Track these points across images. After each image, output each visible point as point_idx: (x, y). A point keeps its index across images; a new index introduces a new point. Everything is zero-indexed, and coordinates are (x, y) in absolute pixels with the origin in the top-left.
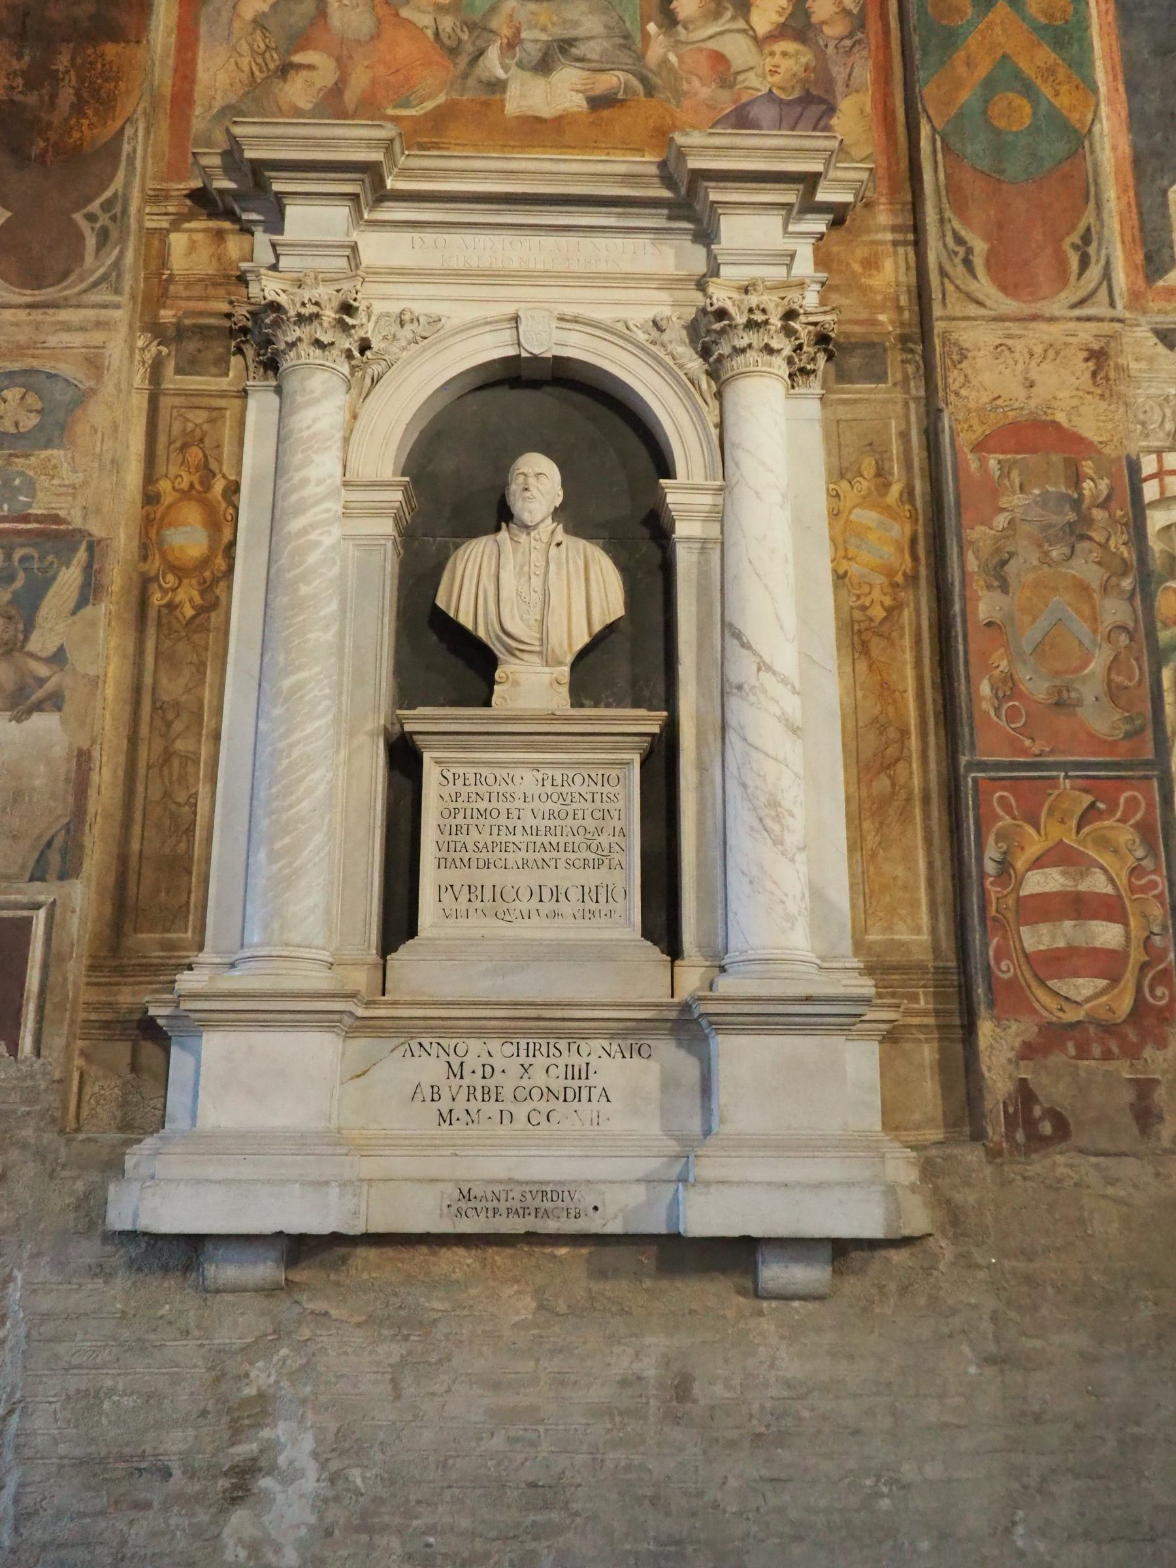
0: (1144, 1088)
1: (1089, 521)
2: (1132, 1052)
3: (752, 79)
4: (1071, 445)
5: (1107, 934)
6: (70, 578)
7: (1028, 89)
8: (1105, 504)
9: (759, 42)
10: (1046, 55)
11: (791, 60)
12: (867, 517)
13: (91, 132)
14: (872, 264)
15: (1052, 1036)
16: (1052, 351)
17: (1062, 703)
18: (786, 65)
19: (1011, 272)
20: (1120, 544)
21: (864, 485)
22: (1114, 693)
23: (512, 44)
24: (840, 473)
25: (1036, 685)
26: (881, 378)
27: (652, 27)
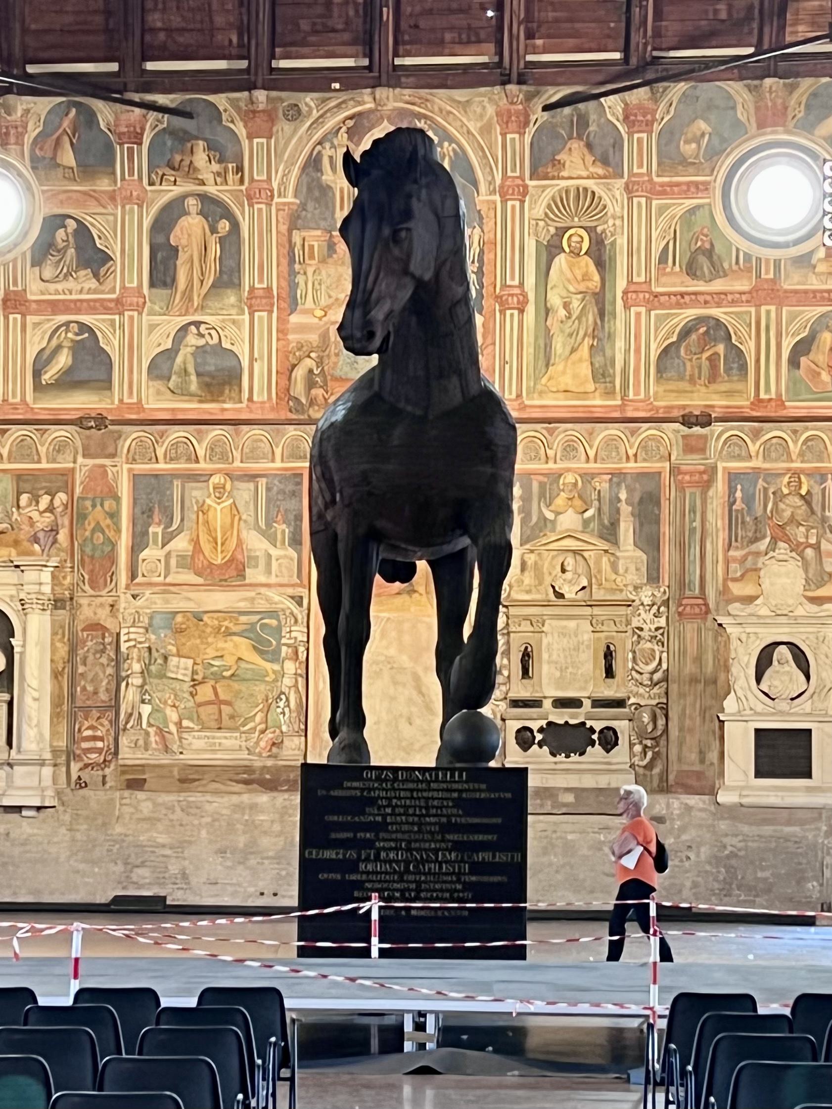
0: (104, 777)
1: (105, 648)
2: (103, 769)
3: (38, 524)
4: (104, 629)
5: (100, 744)
7: (103, 532)
8: (110, 644)
9: (41, 513)
10: (108, 521)
11: (48, 518)
12: (59, 645)
14: (64, 578)
16: (102, 605)
17: (96, 693)
18: (48, 520)
20: (113, 655)
21: (59, 637)
22: (107, 690)
24: (54, 634)
25: (90, 688)
26: (64, 608)
27: (14, 510)
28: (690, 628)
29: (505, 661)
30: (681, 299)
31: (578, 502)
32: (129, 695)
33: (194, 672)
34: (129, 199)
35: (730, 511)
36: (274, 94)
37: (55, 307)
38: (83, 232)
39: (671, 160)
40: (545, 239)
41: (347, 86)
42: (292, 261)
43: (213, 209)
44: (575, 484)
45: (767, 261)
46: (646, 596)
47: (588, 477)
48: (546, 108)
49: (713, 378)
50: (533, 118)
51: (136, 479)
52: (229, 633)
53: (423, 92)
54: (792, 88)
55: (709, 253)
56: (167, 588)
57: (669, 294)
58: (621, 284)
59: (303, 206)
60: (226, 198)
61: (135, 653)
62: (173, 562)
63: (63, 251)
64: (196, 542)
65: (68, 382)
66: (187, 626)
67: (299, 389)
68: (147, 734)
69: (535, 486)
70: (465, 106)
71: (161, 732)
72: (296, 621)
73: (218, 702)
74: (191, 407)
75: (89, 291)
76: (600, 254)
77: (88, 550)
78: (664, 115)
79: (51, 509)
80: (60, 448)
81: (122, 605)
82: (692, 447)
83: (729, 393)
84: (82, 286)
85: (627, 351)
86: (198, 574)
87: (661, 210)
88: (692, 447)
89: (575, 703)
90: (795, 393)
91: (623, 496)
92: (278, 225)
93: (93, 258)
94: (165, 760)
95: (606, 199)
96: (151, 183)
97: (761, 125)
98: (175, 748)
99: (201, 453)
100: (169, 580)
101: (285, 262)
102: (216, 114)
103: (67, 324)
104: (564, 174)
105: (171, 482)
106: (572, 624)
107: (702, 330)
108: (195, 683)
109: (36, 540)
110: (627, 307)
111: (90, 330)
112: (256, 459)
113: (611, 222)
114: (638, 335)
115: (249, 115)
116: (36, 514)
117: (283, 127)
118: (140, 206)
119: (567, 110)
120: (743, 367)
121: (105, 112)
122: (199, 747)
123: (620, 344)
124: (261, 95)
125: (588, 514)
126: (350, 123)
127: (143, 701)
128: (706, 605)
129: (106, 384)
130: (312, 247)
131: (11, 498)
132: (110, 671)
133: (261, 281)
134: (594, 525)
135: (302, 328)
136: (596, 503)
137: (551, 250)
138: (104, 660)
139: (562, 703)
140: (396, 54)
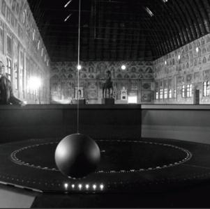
114: (116, 75)
122: (92, 97)
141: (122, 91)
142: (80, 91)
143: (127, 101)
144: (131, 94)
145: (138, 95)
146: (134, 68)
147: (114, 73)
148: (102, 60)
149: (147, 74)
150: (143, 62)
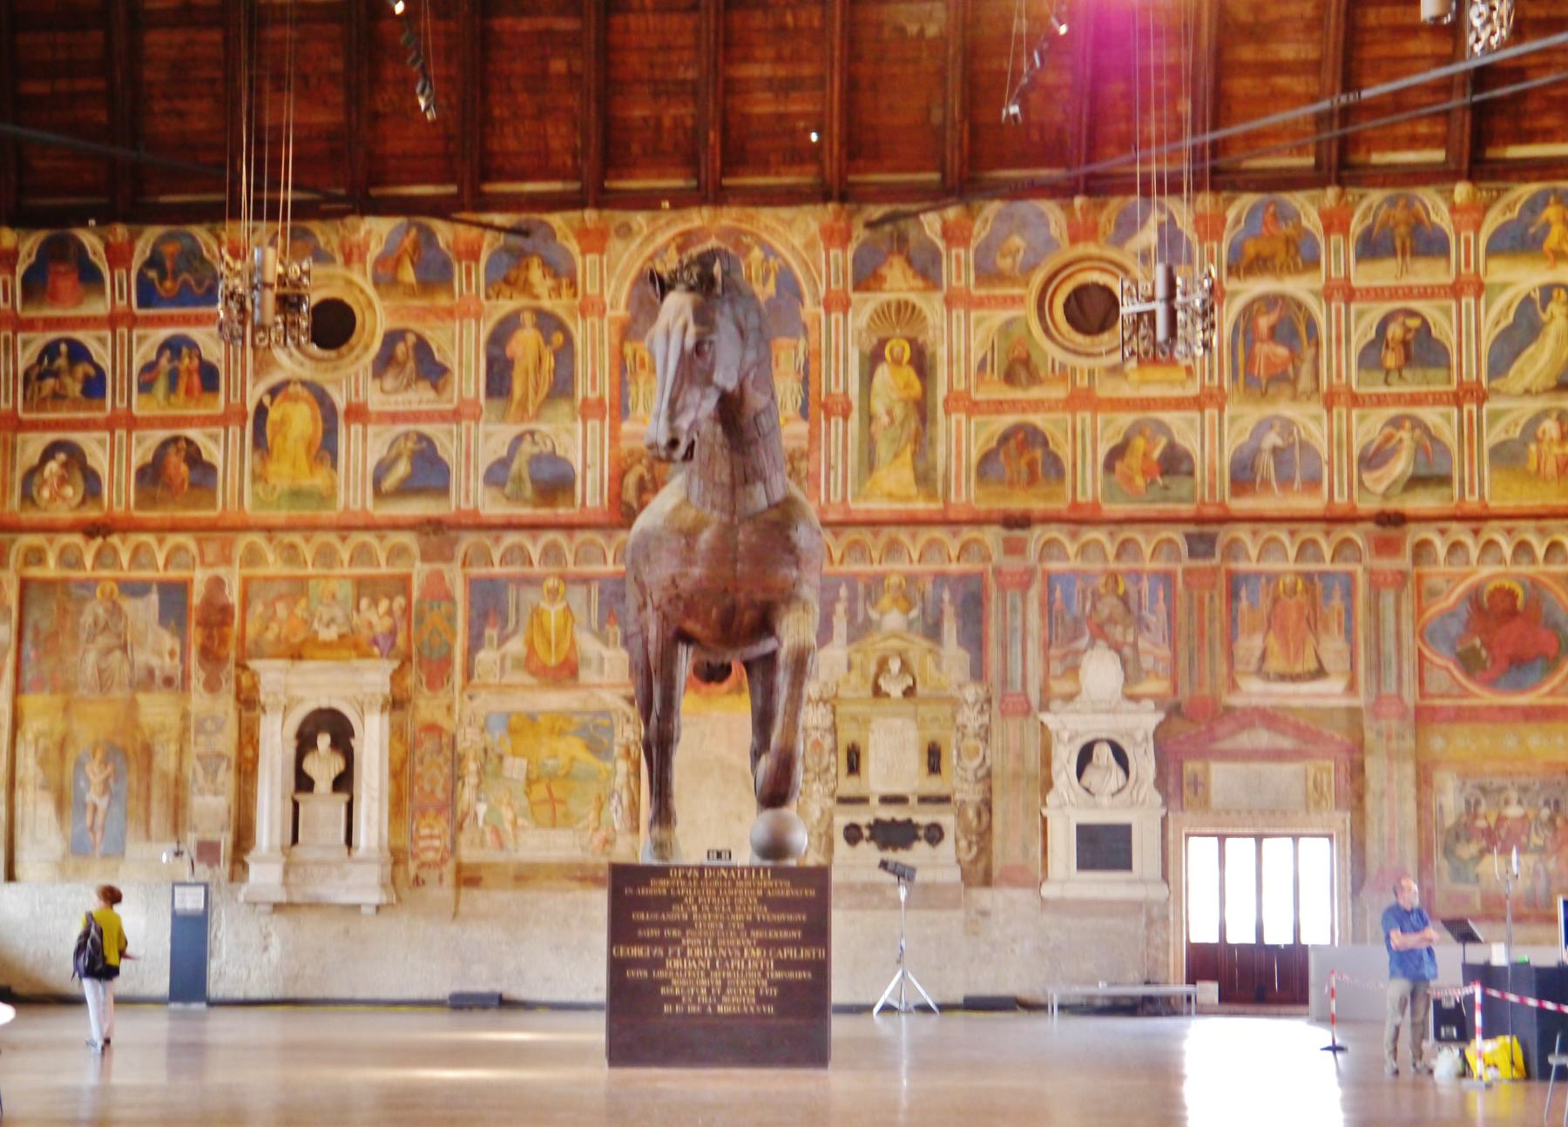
5: (437, 843)
6: (224, 765)
13: (223, 652)
15: (423, 865)
17: (433, 792)
19: (431, 685)
20: (449, 754)
23: (320, 619)
25: (427, 787)
28: (1013, 725)
29: (833, 759)
30: (999, 407)
31: (902, 603)
32: (467, 794)
33: (528, 772)
34: (466, 314)
35: (1050, 611)
36: (606, 213)
37: (394, 417)
38: (422, 347)
39: (988, 275)
40: (868, 348)
41: (676, 206)
42: (623, 369)
43: (548, 323)
44: (900, 586)
45: (1082, 371)
46: (971, 692)
47: (911, 579)
48: (870, 225)
49: (1032, 479)
50: (855, 234)
51: (473, 584)
52: (562, 733)
53: (751, 210)
54: (1102, 206)
55: (1026, 362)
56: (503, 689)
57: (988, 402)
58: (941, 391)
59: (634, 319)
60: (561, 313)
61: (471, 755)
62: (508, 663)
63: (403, 365)
64: (530, 646)
65: (406, 490)
66: (523, 726)
67: (630, 494)
68: (483, 832)
69: (861, 588)
70: (789, 224)
71: (496, 831)
72: (628, 720)
73: (552, 800)
74: (525, 512)
75: (428, 402)
76: (921, 363)
77: (426, 652)
78: (980, 230)
79: (390, 612)
80: (398, 553)
81: (457, 708)
82: (1014, 548)
83: (1048, 497)
84: (420, 397)
85: (948, 456)
86: (533, 673)
87: (979, 322)
88: (1014, 548)
89: (899, 800)
90: (1111, 498)
91: (946, 596)
92: (609, 336)
93: (431, 370)
94: (499, 857)
95: (927, 311)
96: (488, 297)
97: (1074, 240)
98: (510, 845)
99: (535, 556)
100: (504, 681)
101: (616, 373)
102: (551, 234)
103: (407, 435)
104: (887, 286)
105: (506, 587)
106: (898, 723)
107: (1021, 436)
108: (530, 782)
109: (375, 642)
110: (947, 412)
111: (430, 441)
112: (588, 561)
113: (931, 333)
114: (962, 440)
115: (583, 234)
116: (376, 617)
117: (615, 245)
118: (478, 321)
119: (888, 228)
120: (1060, 473)
121: (444, 232)
123: (941, 450)
124: (590, 215)
125: (915, 613)
126: (679, 240)
127: (479, 799)
128: (1028, 703)
129: (443, 491)
130: (642, 360)
131: (351, 603)
132: (446, 770)
133: (594, 387)
134: (919, 625)
135: (636, 436)
136: (919, 604)
137: (874, 358)
138: (441, 760)
139: (887, 800)
140: (723, 174)
141: (1069, 727)
142: (332, 726)
143: (1162, 914)
144: (1222, 777)
145: (1356, 796)
146: (1292, 326)
147: (922, 409)
148: (715, 196)
149: (1513, 409)
150: (1435, 205)
